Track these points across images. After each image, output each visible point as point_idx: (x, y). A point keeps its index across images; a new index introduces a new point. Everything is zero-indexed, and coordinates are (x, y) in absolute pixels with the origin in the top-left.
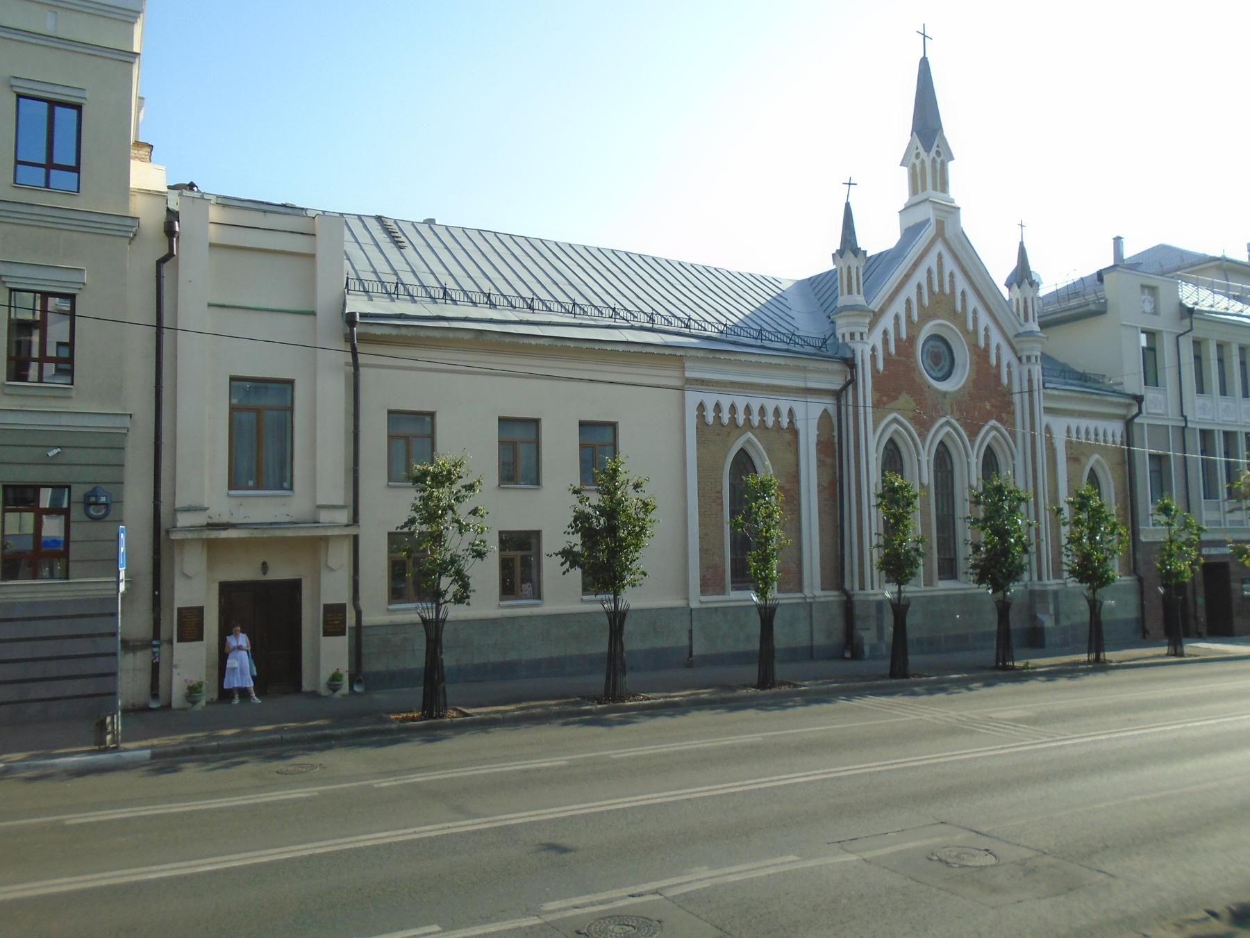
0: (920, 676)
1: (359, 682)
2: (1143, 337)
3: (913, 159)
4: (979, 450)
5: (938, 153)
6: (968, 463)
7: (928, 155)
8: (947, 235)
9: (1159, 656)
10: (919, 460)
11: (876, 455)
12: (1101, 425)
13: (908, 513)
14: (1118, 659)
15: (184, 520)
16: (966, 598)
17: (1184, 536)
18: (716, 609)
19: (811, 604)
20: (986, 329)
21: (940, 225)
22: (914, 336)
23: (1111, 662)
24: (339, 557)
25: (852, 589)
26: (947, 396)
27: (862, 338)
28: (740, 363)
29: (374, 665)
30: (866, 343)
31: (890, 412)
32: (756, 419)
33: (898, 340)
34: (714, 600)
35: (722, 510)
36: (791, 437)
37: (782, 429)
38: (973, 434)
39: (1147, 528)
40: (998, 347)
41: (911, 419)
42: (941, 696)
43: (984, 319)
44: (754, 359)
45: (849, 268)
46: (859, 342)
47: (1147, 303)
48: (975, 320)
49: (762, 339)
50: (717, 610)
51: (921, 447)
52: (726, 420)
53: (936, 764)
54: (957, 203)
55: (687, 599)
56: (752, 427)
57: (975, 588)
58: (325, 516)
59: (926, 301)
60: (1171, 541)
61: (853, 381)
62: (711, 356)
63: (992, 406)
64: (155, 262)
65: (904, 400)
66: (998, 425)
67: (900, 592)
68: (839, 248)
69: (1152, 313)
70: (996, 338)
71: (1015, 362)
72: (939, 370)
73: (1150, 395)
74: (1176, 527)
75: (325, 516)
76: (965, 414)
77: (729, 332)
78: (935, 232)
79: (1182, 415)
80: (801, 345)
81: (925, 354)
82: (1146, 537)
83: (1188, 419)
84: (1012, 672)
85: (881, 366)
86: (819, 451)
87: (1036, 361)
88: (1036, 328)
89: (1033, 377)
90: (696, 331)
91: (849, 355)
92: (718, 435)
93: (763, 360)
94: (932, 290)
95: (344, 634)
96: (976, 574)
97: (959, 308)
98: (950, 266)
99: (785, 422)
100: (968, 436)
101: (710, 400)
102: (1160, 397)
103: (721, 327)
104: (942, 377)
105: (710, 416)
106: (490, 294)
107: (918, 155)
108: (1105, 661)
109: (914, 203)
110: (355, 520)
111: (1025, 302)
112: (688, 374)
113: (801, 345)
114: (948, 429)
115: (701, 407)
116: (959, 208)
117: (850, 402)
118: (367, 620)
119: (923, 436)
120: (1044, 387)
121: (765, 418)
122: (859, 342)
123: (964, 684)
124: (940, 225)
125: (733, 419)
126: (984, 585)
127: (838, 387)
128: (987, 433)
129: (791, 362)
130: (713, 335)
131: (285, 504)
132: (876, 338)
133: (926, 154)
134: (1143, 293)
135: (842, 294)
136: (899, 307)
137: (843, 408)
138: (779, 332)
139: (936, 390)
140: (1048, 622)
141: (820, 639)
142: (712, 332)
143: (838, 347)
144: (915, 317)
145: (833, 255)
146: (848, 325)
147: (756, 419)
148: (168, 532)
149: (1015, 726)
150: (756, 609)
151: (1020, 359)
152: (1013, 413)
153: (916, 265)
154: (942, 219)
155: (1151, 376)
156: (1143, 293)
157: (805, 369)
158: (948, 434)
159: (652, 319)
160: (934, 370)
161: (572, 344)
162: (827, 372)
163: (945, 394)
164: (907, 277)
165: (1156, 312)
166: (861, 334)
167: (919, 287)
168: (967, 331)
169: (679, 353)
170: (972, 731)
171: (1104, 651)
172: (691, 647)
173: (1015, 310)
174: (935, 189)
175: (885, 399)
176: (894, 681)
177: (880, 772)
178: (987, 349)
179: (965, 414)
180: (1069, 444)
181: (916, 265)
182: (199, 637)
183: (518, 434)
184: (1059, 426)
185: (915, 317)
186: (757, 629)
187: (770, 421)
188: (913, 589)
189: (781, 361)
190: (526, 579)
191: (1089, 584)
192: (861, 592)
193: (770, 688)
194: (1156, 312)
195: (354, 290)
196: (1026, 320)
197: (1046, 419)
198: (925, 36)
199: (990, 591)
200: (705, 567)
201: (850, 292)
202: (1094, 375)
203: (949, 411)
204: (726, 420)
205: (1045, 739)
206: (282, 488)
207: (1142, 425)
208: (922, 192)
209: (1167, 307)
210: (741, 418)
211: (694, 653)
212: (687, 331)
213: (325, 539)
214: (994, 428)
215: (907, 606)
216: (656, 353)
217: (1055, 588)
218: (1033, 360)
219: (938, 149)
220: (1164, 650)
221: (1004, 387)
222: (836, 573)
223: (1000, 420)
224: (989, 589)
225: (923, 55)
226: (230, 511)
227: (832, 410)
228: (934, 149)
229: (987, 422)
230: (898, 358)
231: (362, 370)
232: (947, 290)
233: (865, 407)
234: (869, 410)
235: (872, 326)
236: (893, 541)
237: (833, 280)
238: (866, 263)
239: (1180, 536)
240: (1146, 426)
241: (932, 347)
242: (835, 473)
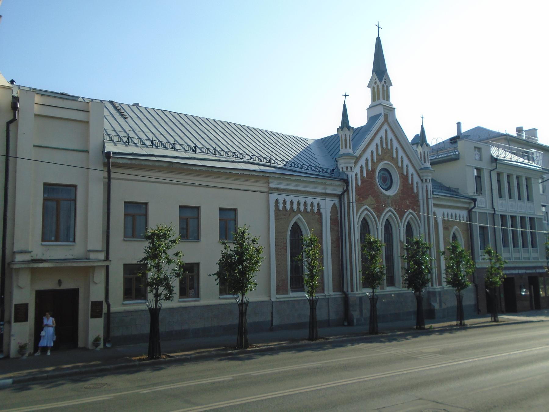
0: (383, 333)
1: (109, 342)
2: (475, 171)
3: (373, 85)
4: (404, 223)
5: (385, 82)
6: (399, 230)
7: (381, 83)
8: (389, 121)
9: (487, 322)
10: (377, 229)
11: (403, 229)
12: (458, 212)
13: (377, 254)
14: (470, 323)
15: (19, 258)
16: (399, 295)
17: (498, 265)
18: (284, 301)
19: (328, 298)
20: (407, 166)
21: (386, 116)
22: (375, 169)
23: (467, 325)
24: (99, 277)
25: (347, 292)
26: (390, 198)
27: (351, 170)
28: (295, 180)
29: (116, 333)
30: (353, 172)
31: (364, 205)
32: (302, 208)
33: (367, 170)
34: (283, 297)
35: (286, 252)
36: (318, 217)
37: (314, 213)
38: (401, 216)
39: (479, 261)
40: (412, 175)
41: (373, 208)
42: (394, 343)
43: (406, 162)
44: (302, 179)
45: (345, 135)
46: (350, 171)
47: (477, 155)
48: (402, 161)
49: (304, 169)
50: (284, 302)
52: (288, 208)
53: (407, 373)
54: (394, 106)
55: (270, 296)
56: (300, 212)
57: (406, 290)
58: (92, 256)
59: (380, 152)
60: (492, 267)
61: (347, 190)
62: (282, 177)
63: (410, 203)
64: (6, 123)
65: (370, 199)
66: (412, 211)
67: (373, 292)
68: (340, 126)
69: (479, 160)
70: (411, 170)
71: (420, 182)
72: (386, 185)
73: (479, 198)
74: (493, 261)
75: (92, 256)
76: (398, 206)
77: (289, 165)
78: (384, 119)
79: (493, 208)
80: (322, 172)
81: (379, 177)
82: (478, 265)
83: (496, 210)
84: (425, 331)
85: (359, 183)
86: (331, 224)
87: (429, 181)
88: (429, 165)
89: (428, 189)
90: (265, 163)
91: (345, 178)
92: (285, 215)
93: (306, 179)
94: (383, 147)
95: (101, 316)
96: (407, 283)
97: (395, 156)
98: (390, 135)
99: (316, 209)
100: (399, 217)
101: (281, 198)
102: (483, 199)
103: (285, 163)
104: (388, 188)
105: (281, 206)
106: (152, 140)
107: (375, 83)
108: (464, 325)
109: (374, 105)
110: (107, 258)
112: (271, 186)
113: (322, 172)
114: (390, 213)
115: (277, 202)
116: (395, 109)
117: (346, 200)
118: (113, 309)
119: (379, 217)
120: (433, 194)
121: (307, 208)
122: (350, 171)
123: (404, 337)
124: (386, 116)
125: (292, 208)
126: (411, 289)
127: (340, 193)
128: (408, 215)
129: (319, 181)
130: (282, 166)
131: (71, 250)
132: (357, 170)
133: (380, 82)
134: (475, 151)
135: (342, 148)
136: (368, 155)
137: (342, 203)
138: (311, 165)
139: (384, 195)
140: (436, 306)
141: (333, 316)
142: (280, 165)
143: (340, 173)
144: (375, 160)
145: (338, 129)
146: (345, 163)
147: (302, 208)
148: (9, 264)
149: (436, 356)
150: (307, 301)
151: (422, 180)
152: (419, 206)
153: (375, 135)
154: (387, 113)
155: (479, 189)
156: (475, 151)
157: (325, 184)
158: (390, 216)
159: (252, 158)
160: (383, 185)
161: (216, 170)
162: (335, 185)
163: (389, 197)
164: (372, 140)
165: (481, 159)
166: (351, 168)
167: (377, 145)
168: (398, 167)
169: (268, 175)
170: (416, 358)
171: (464, 320)
172: (272, 321)
173: (419, 156)
174: (384, 99)
175: (361, 199)
176: (372, 336)
177: (383, 378)
178: (407, 175)
179: (398, 206)
180: (444, 221)
181: (375, 135)
182: (26, 319)
183: (188, 214)
184: (439, 212)
185: (375, 160)
186: (308, 312)
187: (309, 208)
188: (378, 291)
189: (315, 180)
190: (192, 288)
191: (457, 288)
192: (432, 287)
193: (315, 340)
194: (481, 159)
195: (107, 140)
196: (425, 162)
197: (434, 209)
198: (379, 27)
199: (413, 292)
200: (278, 280)
201: (346, 147)
202: (454, 188)
203: (391, 205)
204: (288, 208)
205: (451, 361)
206: (68, 241)
207: (476, 212)
208: (378, 100)
209: (486, 158)
210: (295, 207)
211: (274, 324)
212: (269, 164)
213: (93, 267)
214: (410, 213)
215: (377, 299)
216: (256, 175)
217: (439, 290)
218: (428, 181)
219: (385, 80)
220: (489, 319)
221: (415, 193)
222: (339, 284)
223: (413, 209)
224: (413, 291)
225: (377, 36)
226: (42, 253)
227: (337, 204)
228: (384, 80)
229: (407, 210)
230: (367, 179)
231: (112, 181)
232: (389, 147)
233: (353, 203)
234: (355, 204)
235: (356, 163)
236: (370, 267)
237: (337, 141)
238: (353, 133)
239: (496, 265)
240: (477, 213)
241: (383, 174)
242: (339, 234)
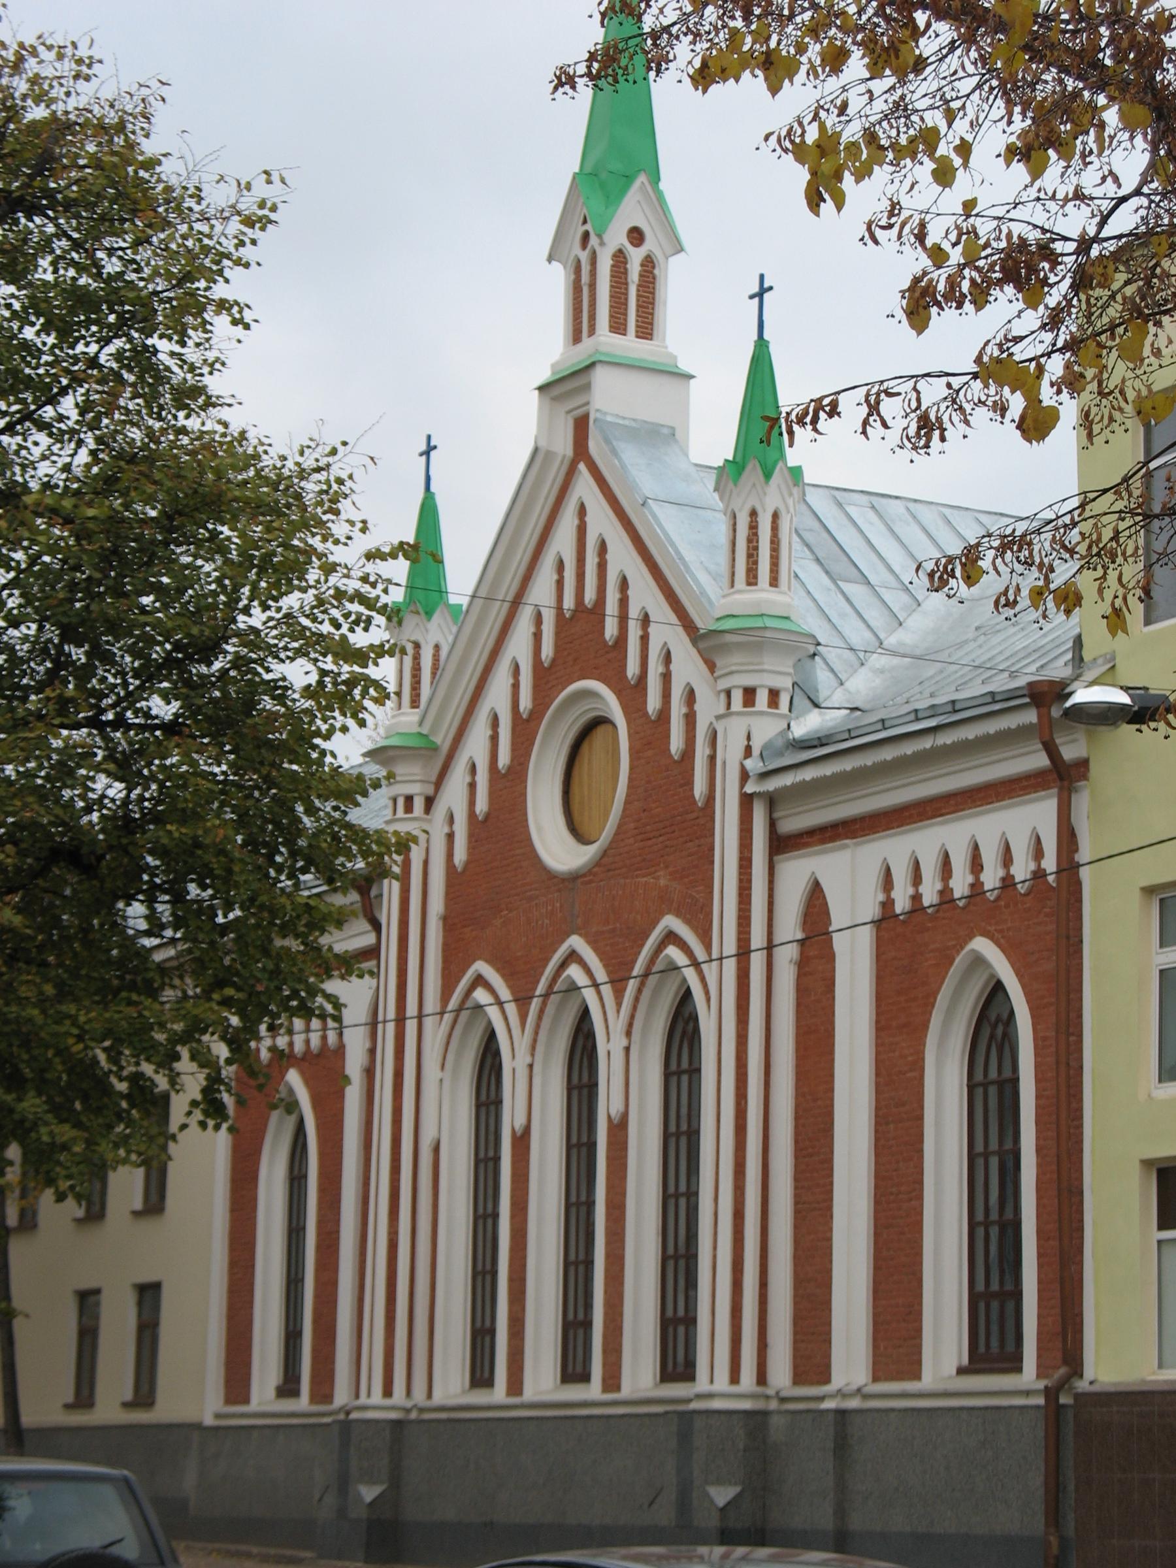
51: (516, 1031)
78: (570, 452)
185: (526, 702)
232: (590, 596)
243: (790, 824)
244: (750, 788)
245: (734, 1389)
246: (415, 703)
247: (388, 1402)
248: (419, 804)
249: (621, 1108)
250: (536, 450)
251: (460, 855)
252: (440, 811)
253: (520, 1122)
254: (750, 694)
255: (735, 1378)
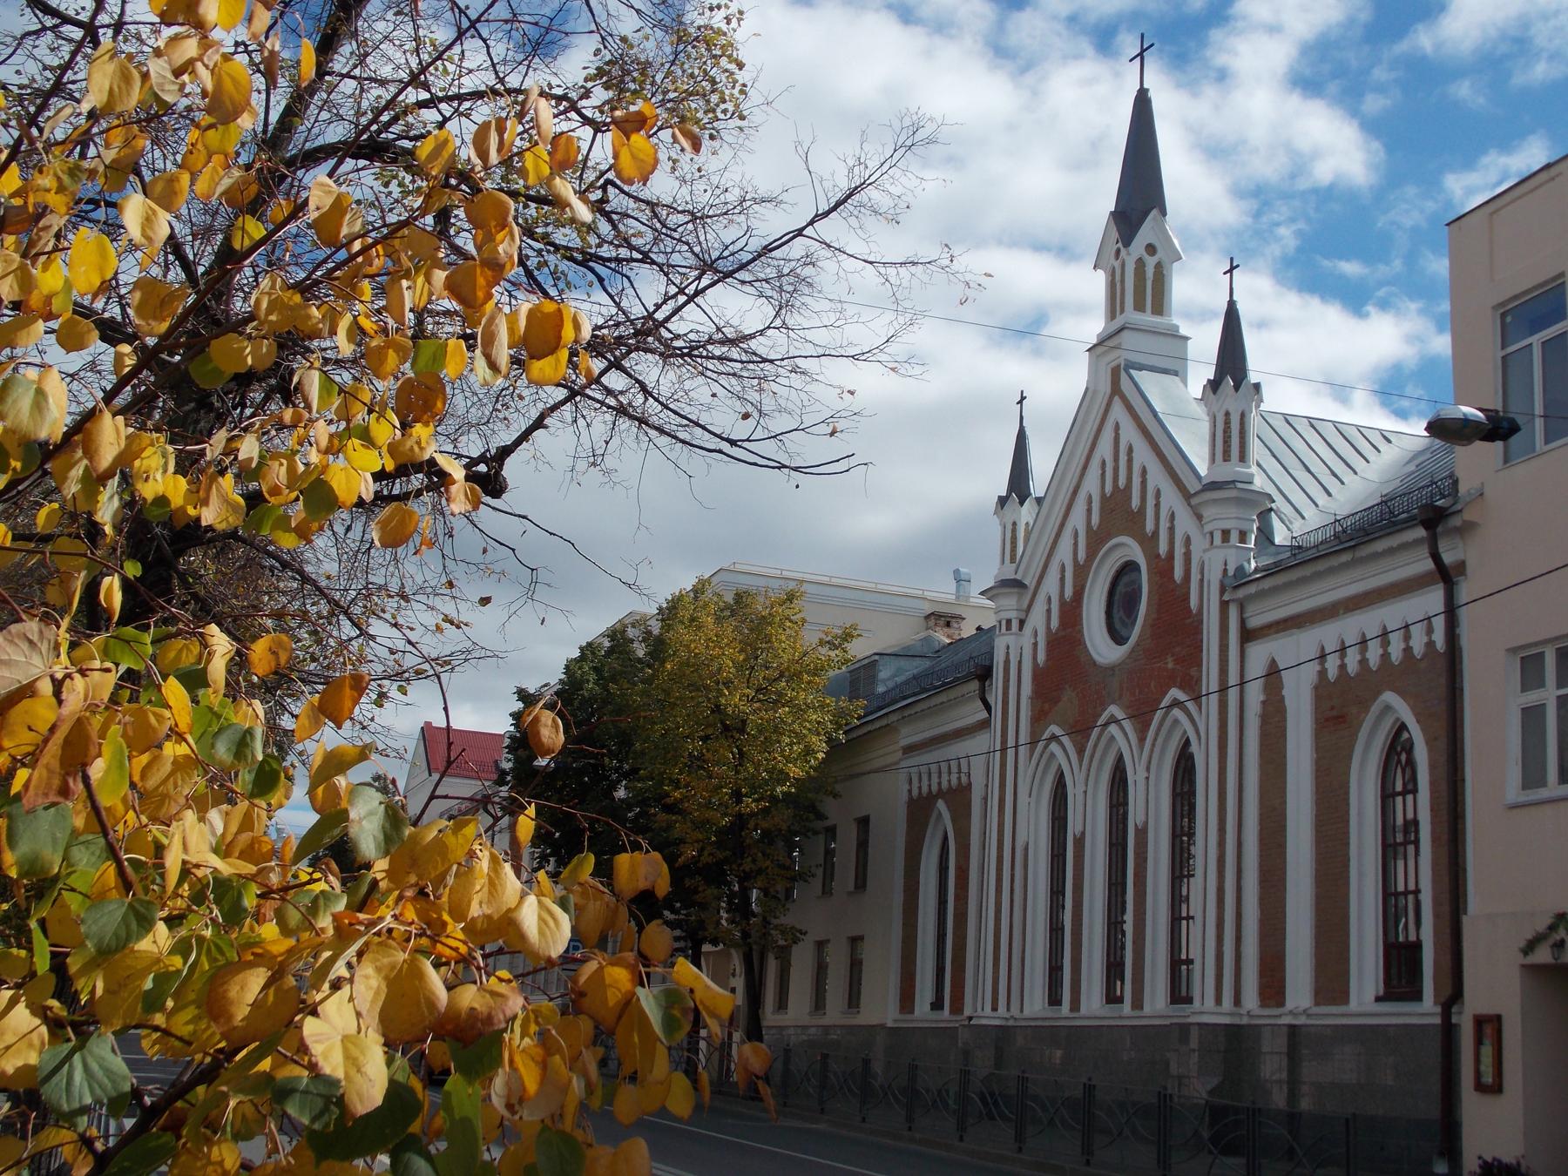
12: (1392, 614)
78: (1109, 391)
111: (1227, 423)
175: (1047, 706)
185: (1082, 555)
232: (1122, 482)
243: (1254, 622)
244: (1226, 598)
245: (1219, 1009)
246: (1013, 560)
247: (994, 1014)
248: (1015, 625)
249: (1143, 819)
250: (1087, 389)
251: (1041, 657)
252: (1028, 629)
253: (1079, 828)
254: (1226, 534)
255: (1218, 1001)
